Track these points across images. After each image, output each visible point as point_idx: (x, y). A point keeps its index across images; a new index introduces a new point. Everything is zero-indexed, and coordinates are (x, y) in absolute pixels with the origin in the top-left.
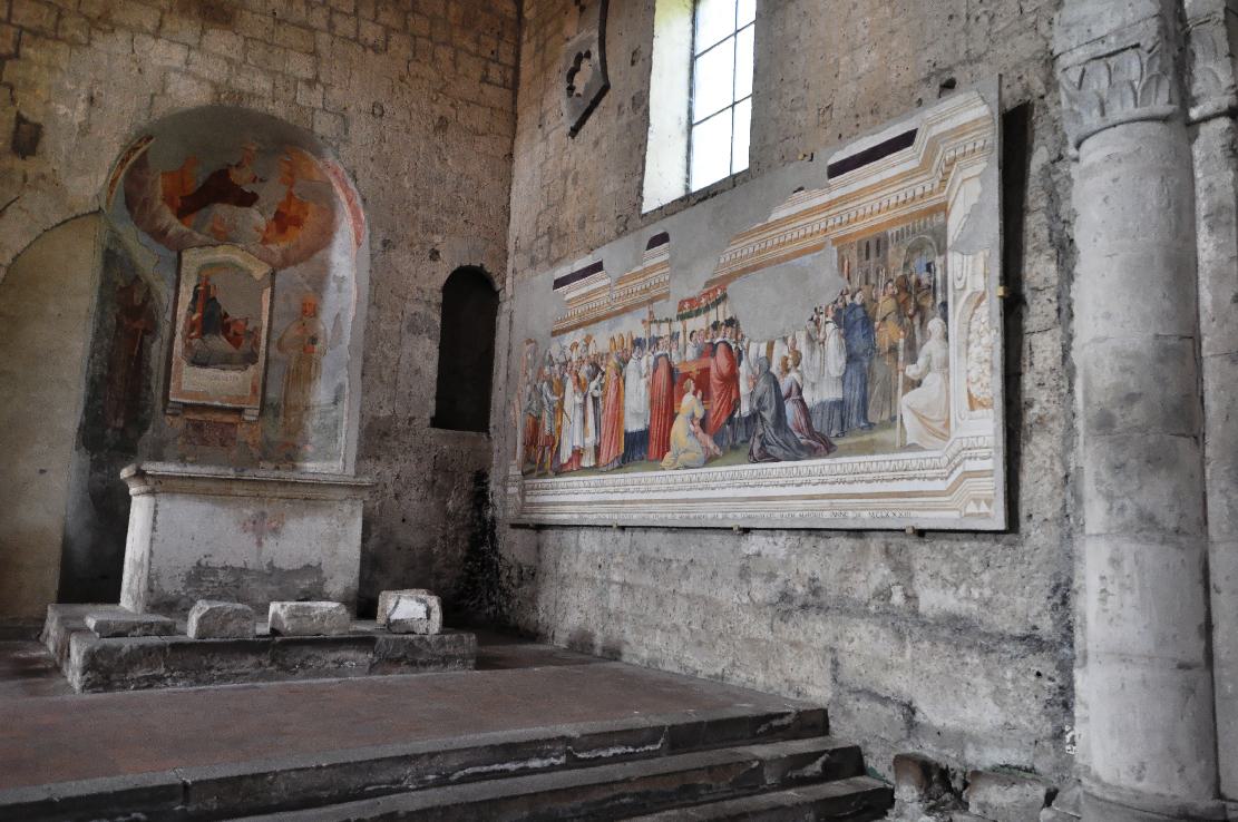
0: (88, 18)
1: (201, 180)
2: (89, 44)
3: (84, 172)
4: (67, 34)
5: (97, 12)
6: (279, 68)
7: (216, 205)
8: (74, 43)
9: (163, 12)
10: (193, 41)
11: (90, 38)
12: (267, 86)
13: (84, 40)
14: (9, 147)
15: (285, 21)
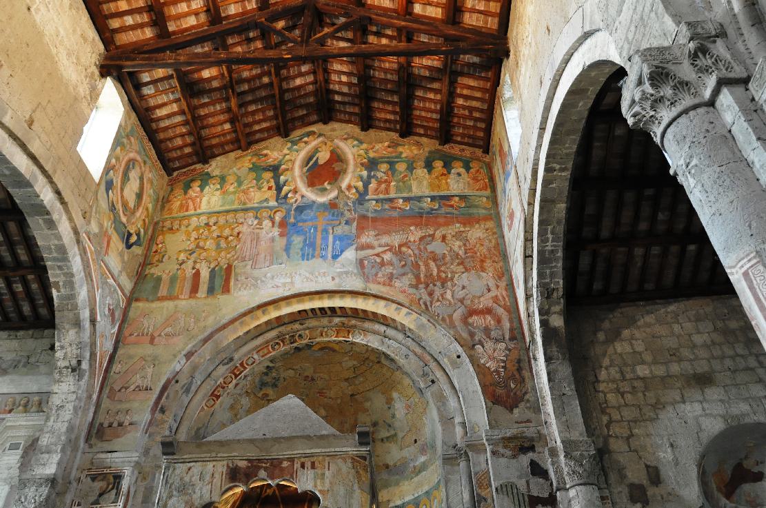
0: (652, 405)
1: (729, 473)
2: (658, 418)
3: (687, 485)
4: (647, 417)
5: (655, 401)
6: (748, 396)
7: (743, 485)
8: (652, 420)
9: (681, 390)
10: (701, 398)
11: (657, 415)
12: (748, 407)
13: (655, 417)
14: (649, 482)
15: (737, 370)
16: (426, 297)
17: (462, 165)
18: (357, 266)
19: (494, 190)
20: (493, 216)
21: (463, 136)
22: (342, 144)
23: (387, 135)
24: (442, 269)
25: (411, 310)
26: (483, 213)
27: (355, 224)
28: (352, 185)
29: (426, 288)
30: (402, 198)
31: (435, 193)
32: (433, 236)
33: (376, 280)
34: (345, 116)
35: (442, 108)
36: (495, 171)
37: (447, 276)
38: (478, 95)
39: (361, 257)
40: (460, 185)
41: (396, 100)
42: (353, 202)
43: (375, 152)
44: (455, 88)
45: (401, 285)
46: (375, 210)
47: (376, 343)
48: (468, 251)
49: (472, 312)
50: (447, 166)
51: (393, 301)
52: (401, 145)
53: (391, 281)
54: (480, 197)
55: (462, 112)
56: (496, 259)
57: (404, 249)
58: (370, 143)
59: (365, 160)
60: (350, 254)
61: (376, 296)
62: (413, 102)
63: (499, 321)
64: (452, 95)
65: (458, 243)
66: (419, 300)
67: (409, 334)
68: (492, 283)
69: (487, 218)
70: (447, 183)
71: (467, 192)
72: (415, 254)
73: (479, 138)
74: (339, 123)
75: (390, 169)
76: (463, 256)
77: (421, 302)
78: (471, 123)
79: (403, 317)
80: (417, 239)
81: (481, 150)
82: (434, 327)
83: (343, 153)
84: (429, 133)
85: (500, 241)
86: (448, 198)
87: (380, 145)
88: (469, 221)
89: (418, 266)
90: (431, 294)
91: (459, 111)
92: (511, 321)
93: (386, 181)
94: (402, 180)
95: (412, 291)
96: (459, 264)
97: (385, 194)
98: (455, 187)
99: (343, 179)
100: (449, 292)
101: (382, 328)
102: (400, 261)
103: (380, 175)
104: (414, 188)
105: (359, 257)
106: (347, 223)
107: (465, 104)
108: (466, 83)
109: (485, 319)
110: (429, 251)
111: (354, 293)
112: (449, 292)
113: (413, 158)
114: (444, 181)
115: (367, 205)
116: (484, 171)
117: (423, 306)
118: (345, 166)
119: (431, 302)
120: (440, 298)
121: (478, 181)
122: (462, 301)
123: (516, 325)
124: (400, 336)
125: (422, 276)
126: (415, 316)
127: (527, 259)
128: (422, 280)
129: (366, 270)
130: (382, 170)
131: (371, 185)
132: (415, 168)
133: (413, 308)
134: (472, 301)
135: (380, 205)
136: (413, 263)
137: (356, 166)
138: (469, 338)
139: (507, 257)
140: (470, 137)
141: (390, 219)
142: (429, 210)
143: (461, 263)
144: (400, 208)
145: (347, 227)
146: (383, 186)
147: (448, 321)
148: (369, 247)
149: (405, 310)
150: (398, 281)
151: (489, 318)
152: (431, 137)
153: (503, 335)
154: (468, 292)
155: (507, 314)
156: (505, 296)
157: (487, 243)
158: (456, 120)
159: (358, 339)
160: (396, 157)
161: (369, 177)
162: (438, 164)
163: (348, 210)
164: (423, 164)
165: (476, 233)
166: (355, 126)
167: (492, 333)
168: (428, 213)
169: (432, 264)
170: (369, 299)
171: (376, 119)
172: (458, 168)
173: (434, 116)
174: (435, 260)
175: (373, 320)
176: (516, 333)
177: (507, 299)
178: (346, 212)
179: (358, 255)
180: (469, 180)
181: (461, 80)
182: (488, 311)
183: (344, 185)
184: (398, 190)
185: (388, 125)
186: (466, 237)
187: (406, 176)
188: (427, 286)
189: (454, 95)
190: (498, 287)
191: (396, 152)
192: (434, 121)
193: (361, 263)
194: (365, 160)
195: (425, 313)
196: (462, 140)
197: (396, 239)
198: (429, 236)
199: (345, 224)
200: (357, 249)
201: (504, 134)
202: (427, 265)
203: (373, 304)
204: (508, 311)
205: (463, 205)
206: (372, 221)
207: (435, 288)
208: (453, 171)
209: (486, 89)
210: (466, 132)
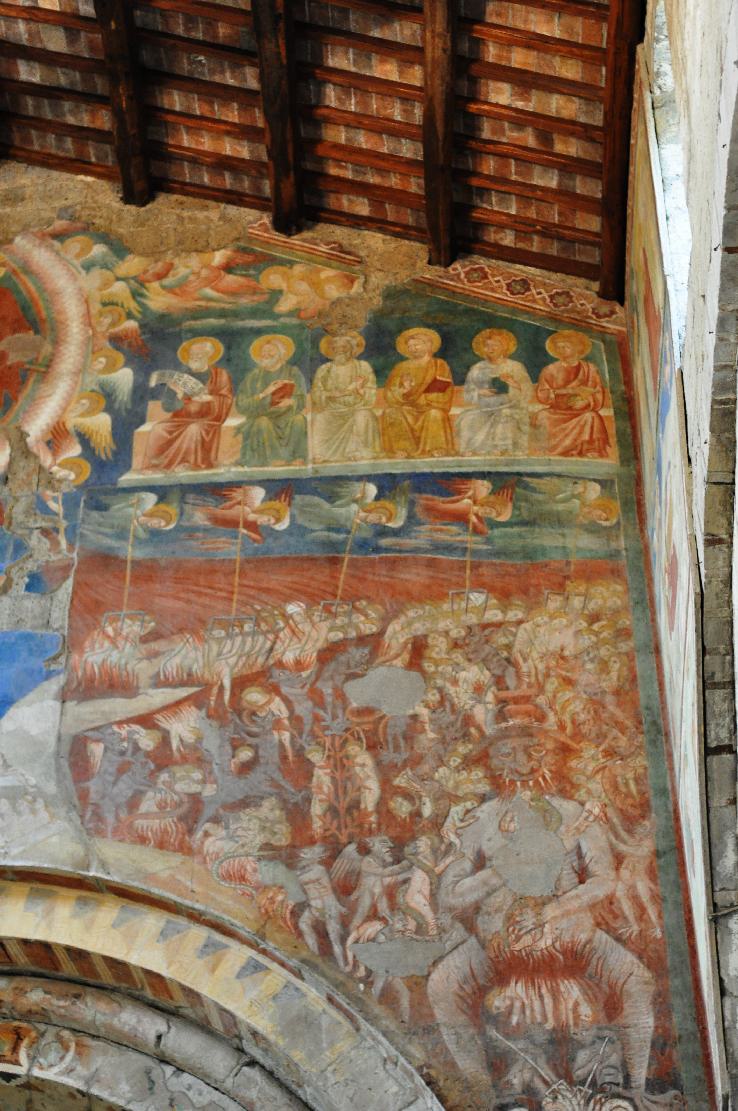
16: (324, 902)
17: (513, 348)
18: (58, 769)
19: (632, 450)
20: (623, 561)
21: (523, 227)
22: (42, 257)
23: (223, 217)
24: (400, 781)
25: (264, 952)
26: (579, 550)
27: (69, 584)
28: (70, 425)
29: (328, 863)
30: (261, 483)
31: (398, 465)
32: (373, 643)
33: (131, 826)
34: (60, 138)
35: (429, 116)
36: (637, 372)
37: (418, 814)
38: (570, 70)
39: (73, 732)
40: (499, 429)
41: (253, 84)
42: (70, 502)
43: (169, 290)
44: (477, 43)
45: (228, 846)
46: (155, 534)
47: (124, 1087)
48: (511, 707)
49: (506, 968)
50: (455, 350)
51: (195, 917)
52: (272, 261)
53: (191, 831)
54: (576, 479)
55: (511, 135)
56: (623, 742)
57: (254, 696)
58: (153, 253)
59: (132, 324)
60: (38, 716)
61: (123, 893)
62: (320, 95)
63: (612, 1005)
64: (464, 70)
65: (473, 673)
66: (296, 913)
67: (256, 1053)
68: (595, 845)
69: (593, 571)
70: (447, 420)
71: (527, 460)
72: (296, 720)
73: (588, 239)
74: (38, 169)
75: (227, 360)
76: (489, 731)
77: (305, 924)
78: (552, 181)
79: (226, 982)
80: (311, 654)
81: (596, 286)
82: (347, 1025)
83: (43, 290)
84: (391, 217)
85: (642, 665)
86: (448, 483)
87: (195, 261)
88: (524, 580)
89: (305, 769)
90: (345, 889)
91: (502, 132)
92: (661, 1005)
93: (204, 412)
94: (271, 409)
95: (270, 873)
96: (469, 762)
97: (196, 467)
98: (480, 437)
99: (34, 402)
100: (419, 880)
101: (149, 1026)
102: (235, 748)
103: (183, 384)
104: (315, 445)
105: (73, 728)
106: (35, 584)
107: (520, 104)
108: (521, 26)
109: (556, 995)
110: (355, 705)
111: (39, 881)
112: (419, 880)
113: (320, 314)
114: (435, 413)
115: (120, 508)
116: (601, 370)
117: (311, 940)
118: (47, 348)
119: (345, 923)
120: (383, 907)
121: (573, 413)
122: (468, 919)
123: (679, 1022)
124: (219, 1061)
125: (317, 809)
126: (278, 977)
127: (714, 760)
128: (317, 826)
129: (93, 786)
130: (195, 365)
131: (145, 428)
132: (328, 360)
133: (270, 946)
134: (510, 919)
135: (173, 509)
136: (284, 758)
137: (91, 348)
138: (485, 1078)
139: (667, 735)
140: (548, 232)
141: (212, 569)
142: (366, 534)
143: (480, 759)
144: (252, 526)
145: (32, 604)
146: (194, 430)
147: (405, 1002)
148: (116, 685)
149: (238, 954)
150: (224, 833)
151: (572, 990)
152: (402, 232)
153: (625, 1067)
154: (495, 881)
155: (648, 975)
156: (645, 898)
157: (587, 675)
158: (489, 166)
159: (55, 1068)
160: (254, 313)
161: (142, 394)
162: (420, 344)
163: (45, 532)
164: (355, 340)
165: (550, 632)
166: (104, 185)
167: (582, 1056)
168: (363, 545)
169: (363, 761)
170: (99, 903)
171: (182, 158)
172: (497, 358)
173: (409, 149)
174: (372, 747)
175: (114, 990)
176: (676, 1056)
177: (652, 913)
178: (35, 541)
179: (68, 719)
180: (541, 407)
181: (499, 15)
182: (573, 962)
183: (37, 426)
184: (253, 446)
185: (228, 181)
186: (509, 647)
187: (285, 391)
188: (334, 851)
189: (475, 69)
190: (619, 860)
191: (255, 291)
192: (403, 169)
193: (75, 754)
194: (132, 324)
195: (314, 967)
196: (520, 245)
197: (221, 657)
198: (361, 640)
199: (29, 588)
200: (63, 697)
201: (653, 236)
202: (340, 765)
203: (113, 926)
204: (655, 964)
205: (505, 517)
206: (135, 579)
207: (368, 859)
208: (475, 372)
209: (598, 49)
210: (532, 213)
